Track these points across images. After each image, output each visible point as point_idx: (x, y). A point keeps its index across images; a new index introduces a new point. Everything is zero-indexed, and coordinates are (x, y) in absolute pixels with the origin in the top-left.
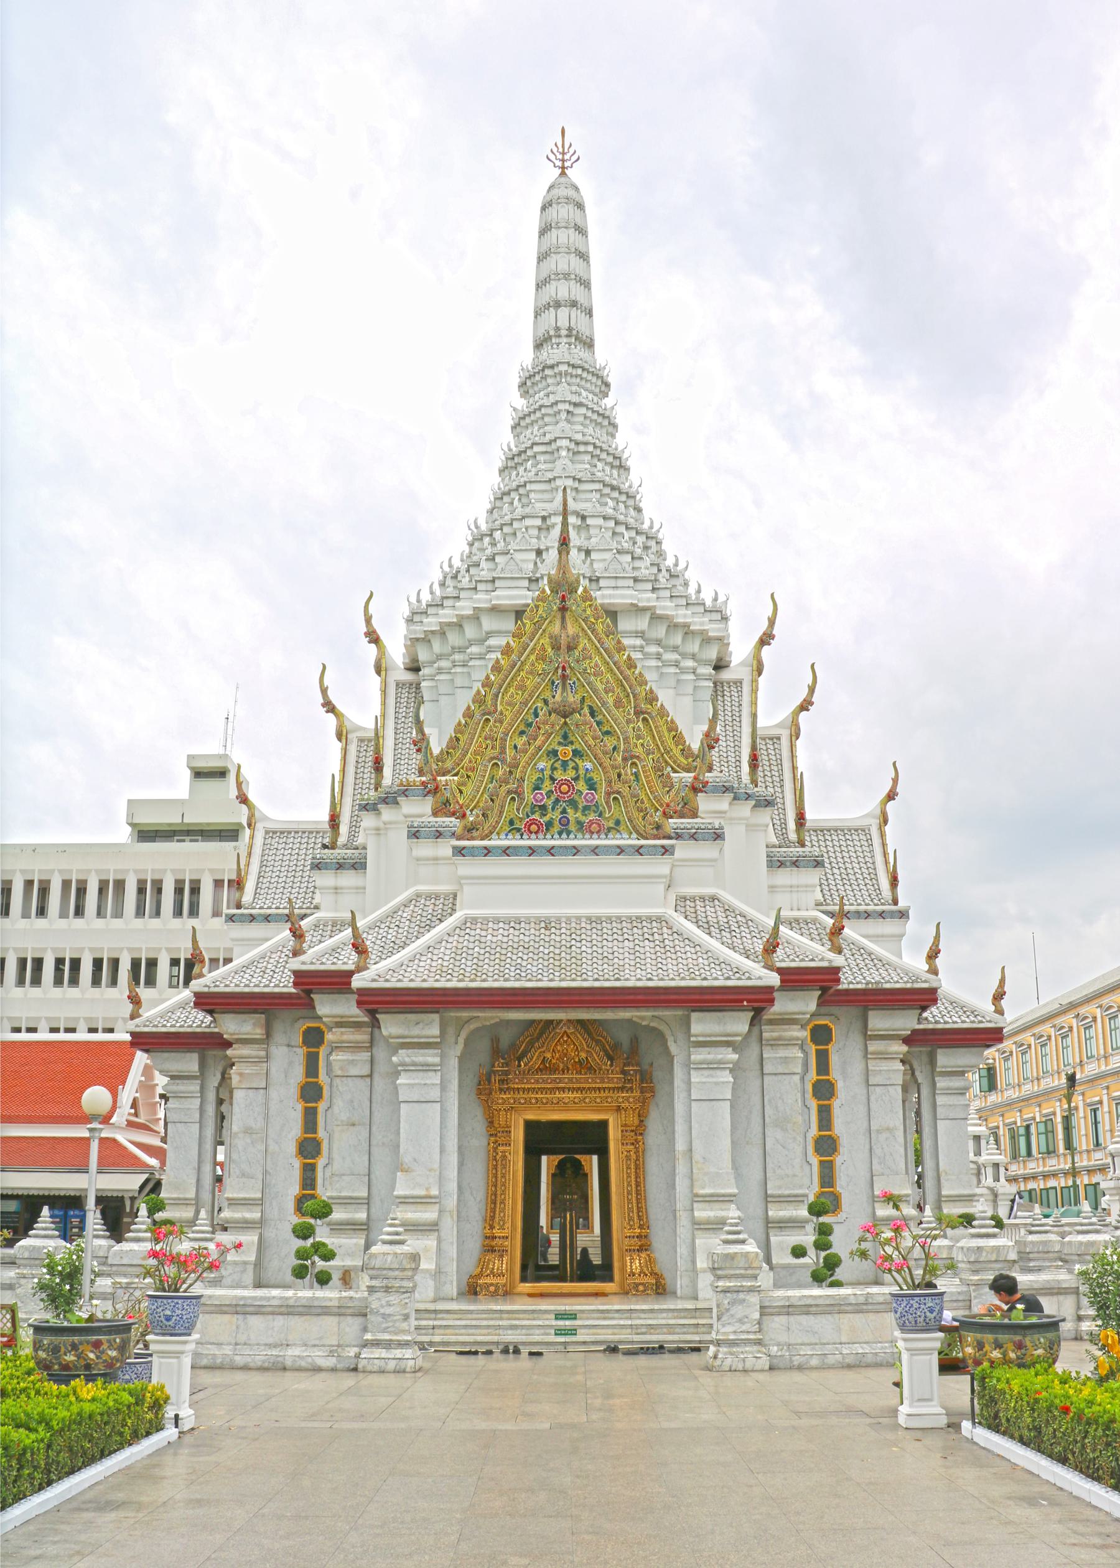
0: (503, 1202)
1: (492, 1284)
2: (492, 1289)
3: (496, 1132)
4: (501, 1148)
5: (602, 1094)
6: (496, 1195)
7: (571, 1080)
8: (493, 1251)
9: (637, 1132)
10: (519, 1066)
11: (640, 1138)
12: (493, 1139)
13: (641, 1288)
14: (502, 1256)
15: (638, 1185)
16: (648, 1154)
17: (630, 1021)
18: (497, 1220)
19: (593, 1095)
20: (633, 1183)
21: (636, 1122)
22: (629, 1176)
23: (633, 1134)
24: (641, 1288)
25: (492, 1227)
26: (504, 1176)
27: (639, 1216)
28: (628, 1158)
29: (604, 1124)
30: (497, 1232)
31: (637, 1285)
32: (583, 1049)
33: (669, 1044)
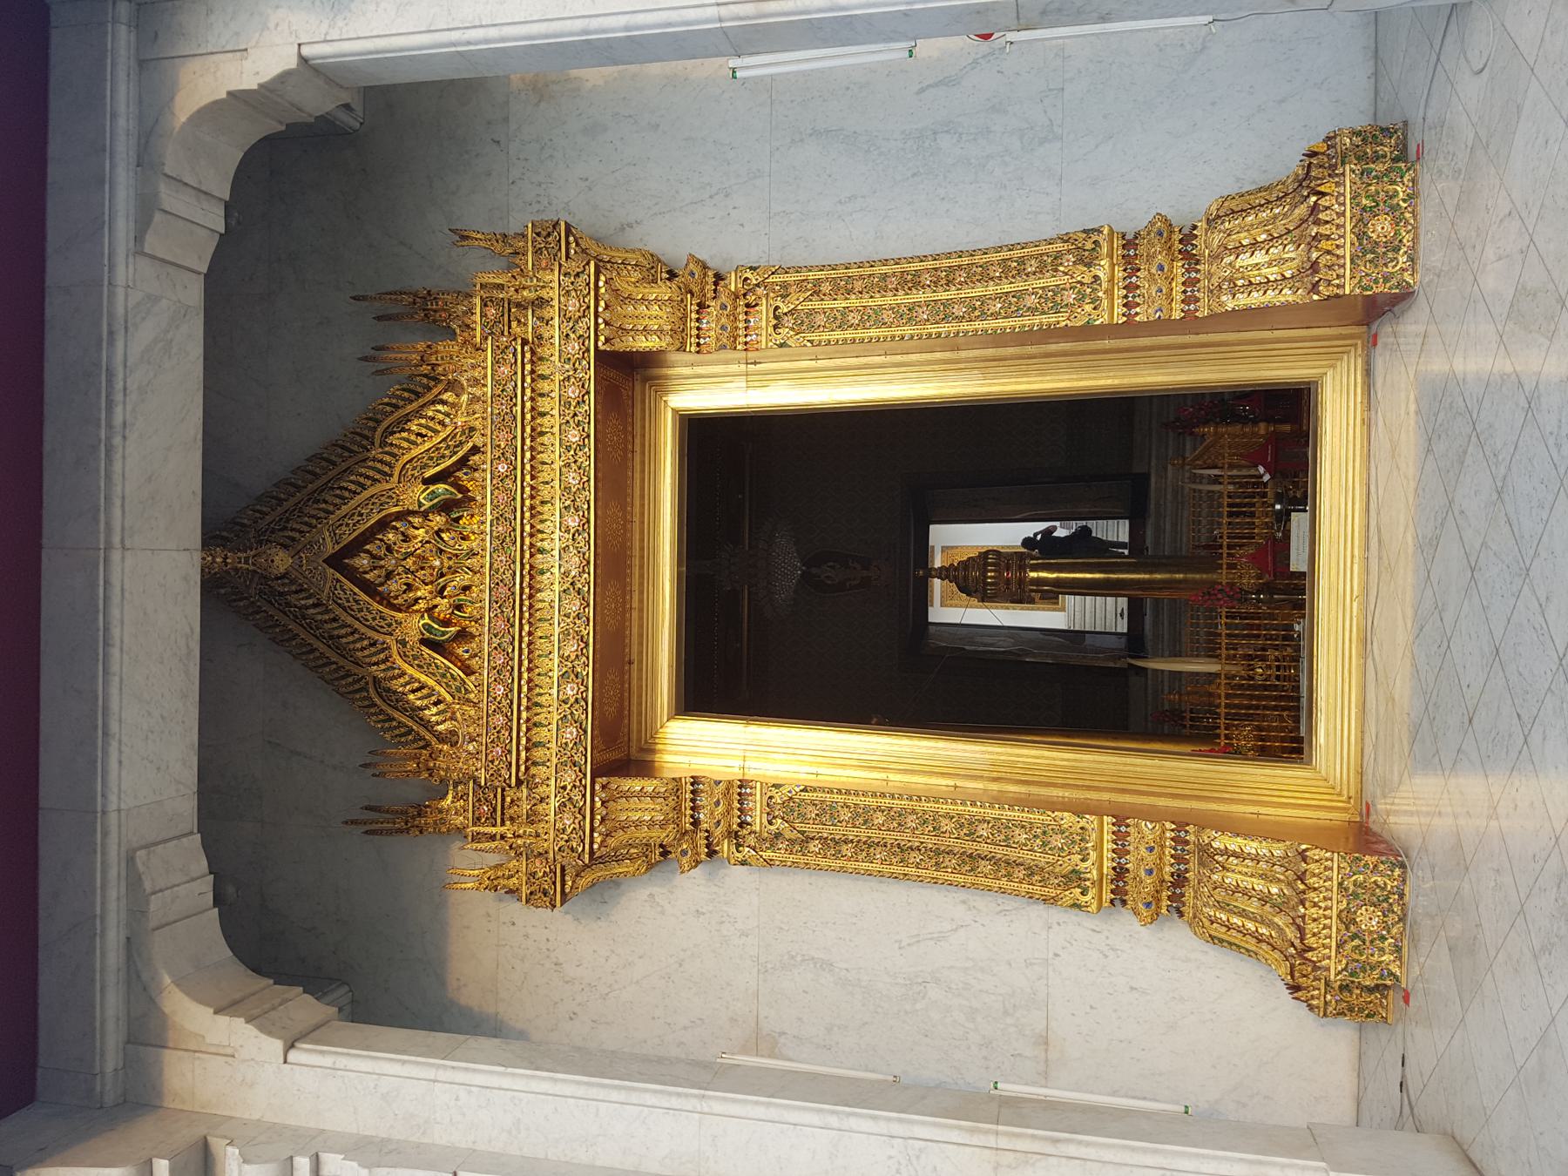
0: (969, 827)
1: (1347, 919)
2: (1368, 919)
3: (710, 829)
4: (757, 819)
5: (552, 422)
6: (938, 852)
7: (501, 542)
8: (1180, 880)
9: (708, 295)
10: (453, 733)
11: (733, 284)
12: (725, 847)
13: (1381, 227)
14: (1207, 854)
15: (912, 282)
16: (798, 256)
17: (238, 295)
18: (1042, 860)
19: (554, 455)
20: (902, 298)
21: (664, 291)
22: (870, 317)
23: (714, 308)
24: (1381, 227)
25: (1074, 878)
26: (863, 816)
27: (1041, 270)
28: (805, 322)
29: (701, 433)
30: (1098, 863)
31: (1367, 248)
32: (390, 495)
33: (250, 83)
